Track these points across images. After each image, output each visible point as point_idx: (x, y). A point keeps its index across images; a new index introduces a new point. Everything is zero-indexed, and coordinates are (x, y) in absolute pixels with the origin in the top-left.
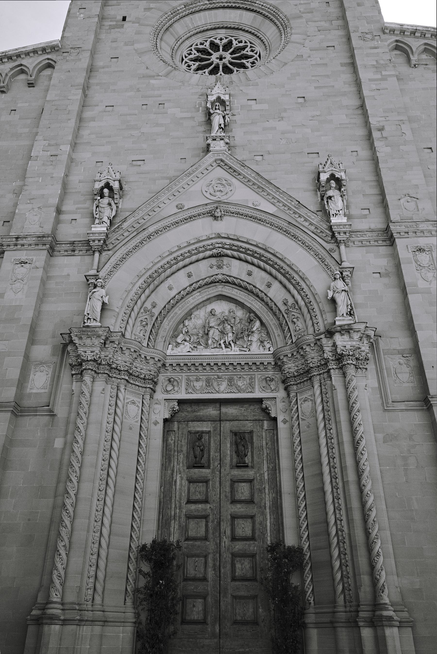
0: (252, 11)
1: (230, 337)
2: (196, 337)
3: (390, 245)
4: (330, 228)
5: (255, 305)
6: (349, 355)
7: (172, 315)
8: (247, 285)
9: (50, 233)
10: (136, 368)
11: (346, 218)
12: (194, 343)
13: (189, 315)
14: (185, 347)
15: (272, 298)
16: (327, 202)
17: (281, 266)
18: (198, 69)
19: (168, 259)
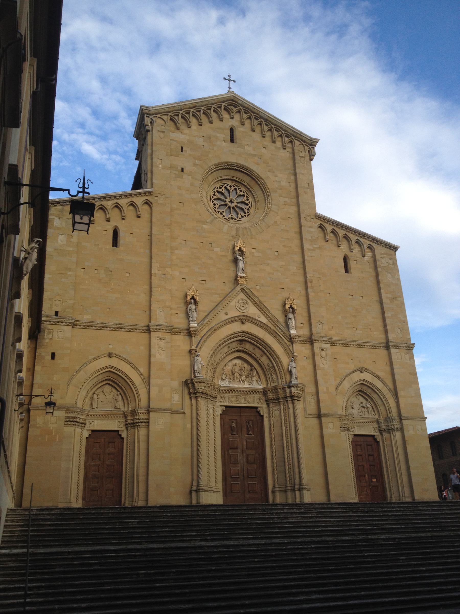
1: (244, 378)
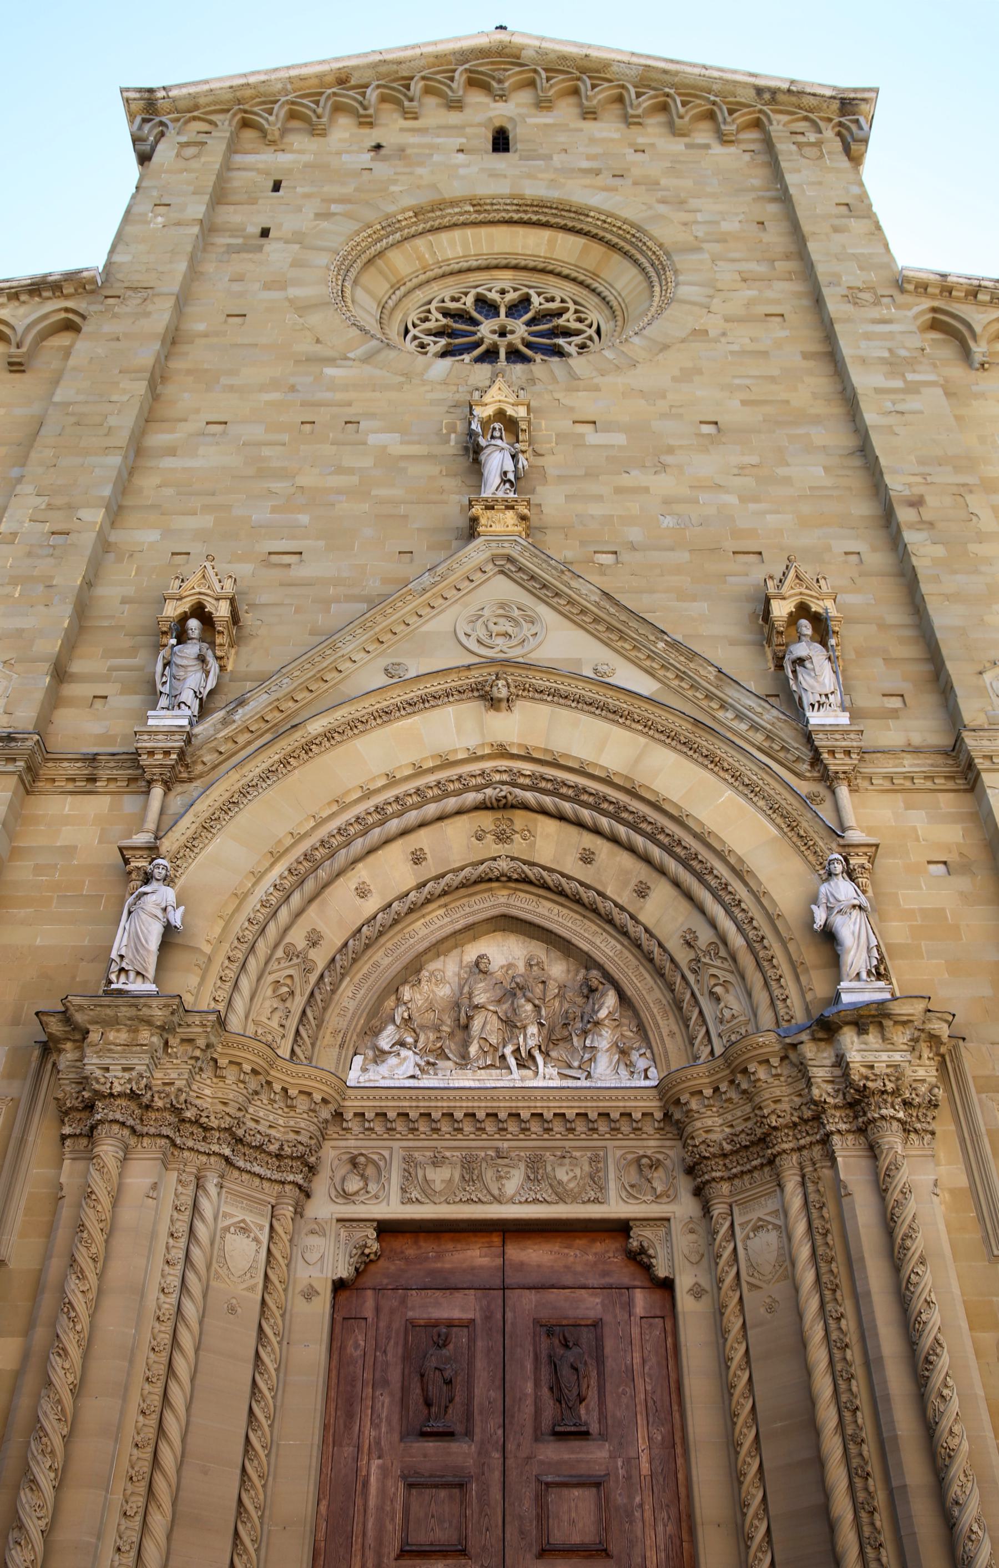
0: (579, 232)
1: (532, 1036)
2: (432, 1036)
3: (965, 791)
4: (808, 738)
5: (602, 946)
6: (883, 1092)
7: (364, 970)
8: (581, 889)
9: (31, 728)
10: (257, 1122)
11: (847, 714)
12: (425, 1052)
13: (412, 970)
14: (401, 1064)
15: (650, 926)
16: (794, 672)
17: (676, 837)
18: (444, 354)
19: (359, 809)
